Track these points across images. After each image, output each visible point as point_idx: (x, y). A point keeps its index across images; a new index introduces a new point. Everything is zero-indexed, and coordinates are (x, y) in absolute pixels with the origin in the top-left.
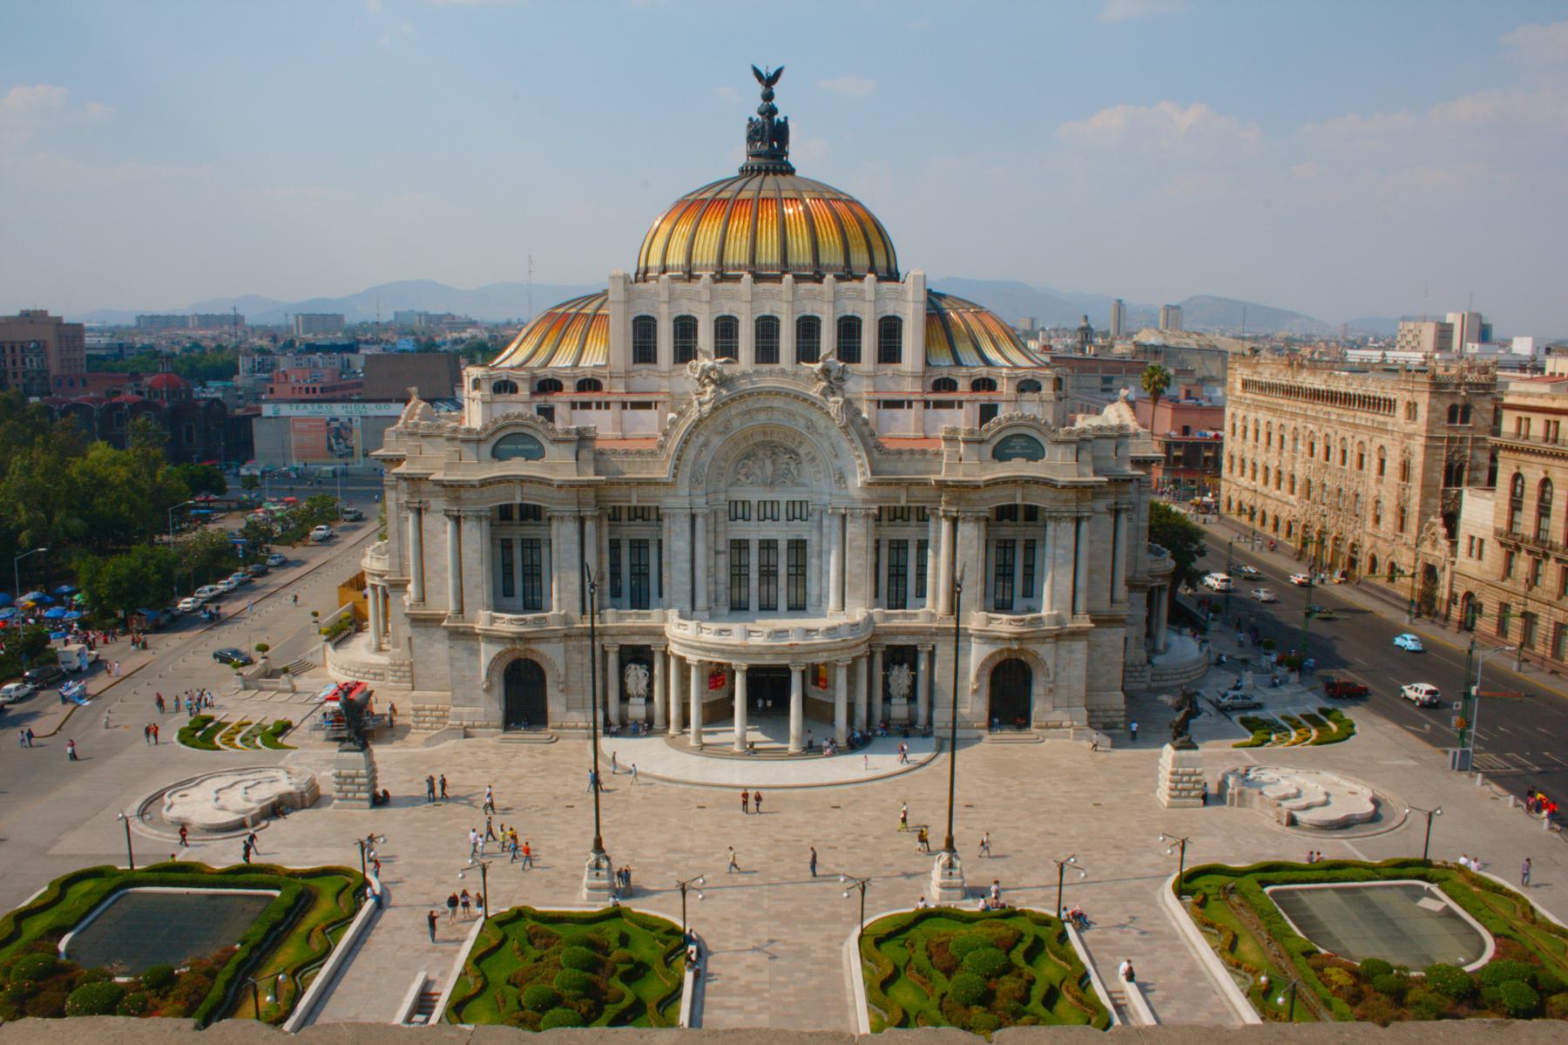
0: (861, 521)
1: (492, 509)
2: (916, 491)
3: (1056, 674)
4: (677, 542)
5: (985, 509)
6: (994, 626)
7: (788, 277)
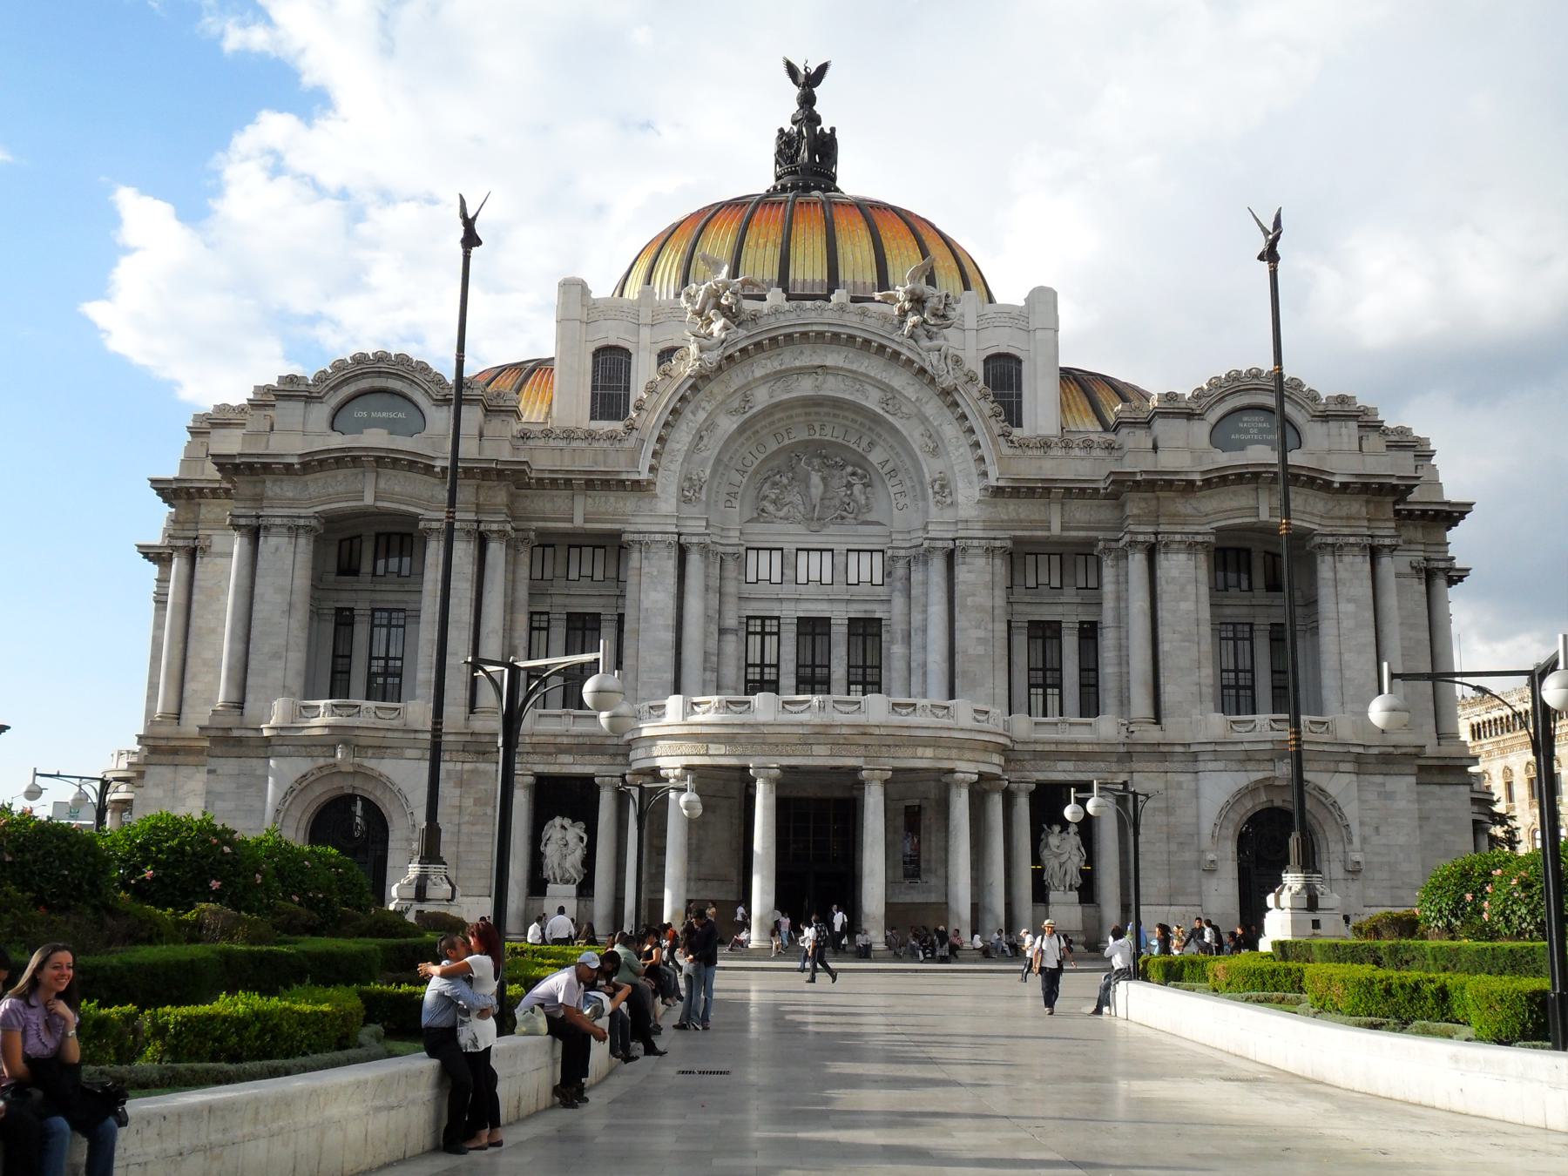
0: (981, 562)
1: (318, 516)
2: (1081, 513)
3: (1364, 840)
4: (651, 591)
5: (1204, 529)
6: (1241, 734)
7: (840, 296)
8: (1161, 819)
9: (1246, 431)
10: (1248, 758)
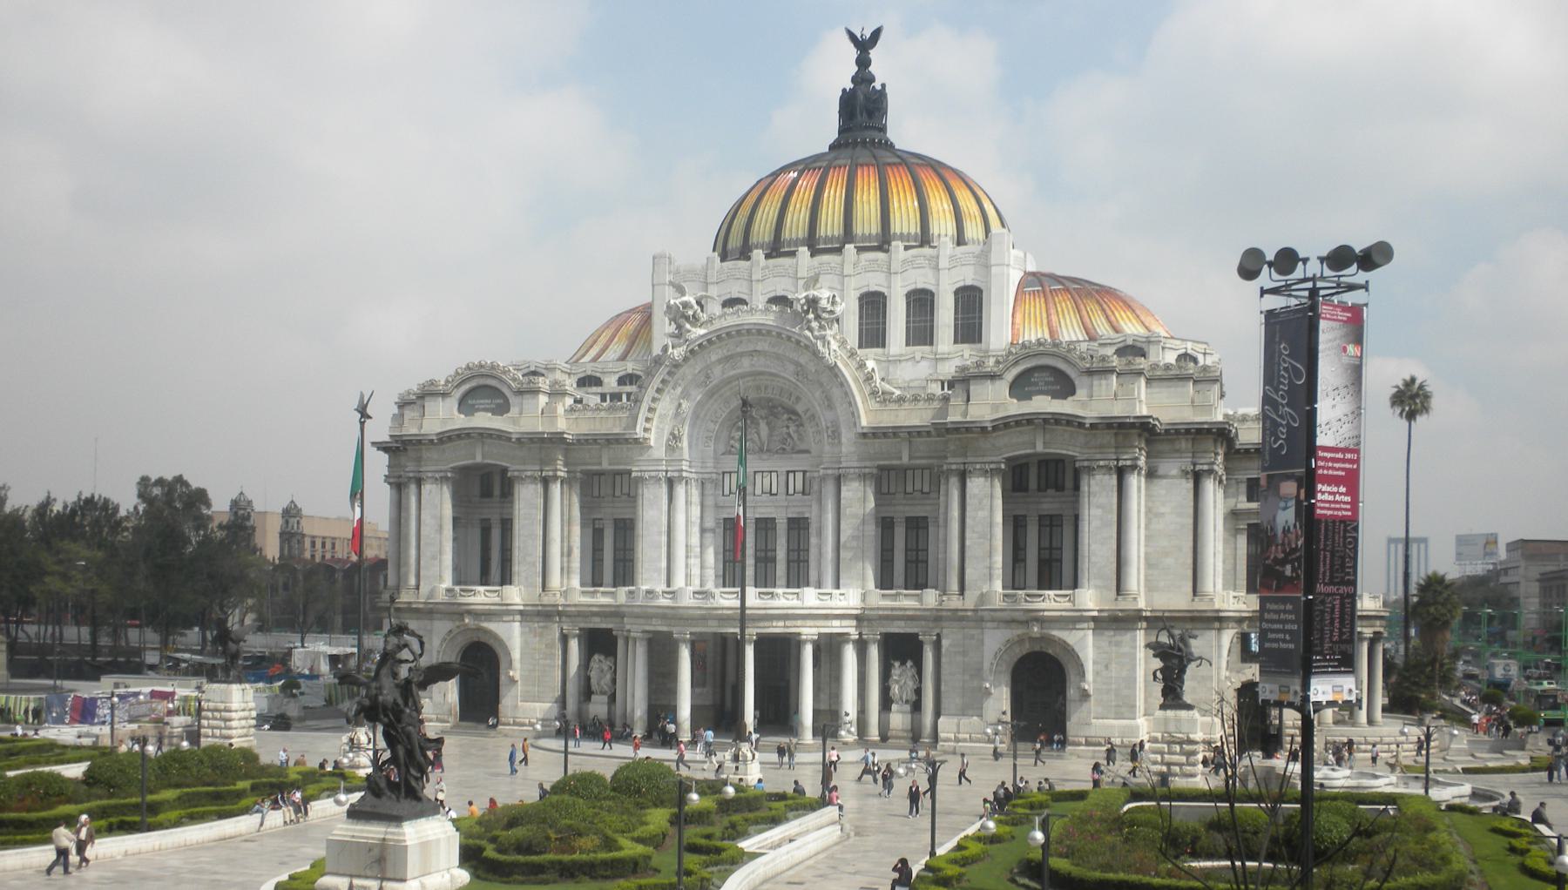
0: (855, 485)
1: (454, 469)
3: (1097, 673)
5: (999, 458)
7: (850, 247)
8: (959, 658)
9: (1036, 384)
10: (1011, 622)
